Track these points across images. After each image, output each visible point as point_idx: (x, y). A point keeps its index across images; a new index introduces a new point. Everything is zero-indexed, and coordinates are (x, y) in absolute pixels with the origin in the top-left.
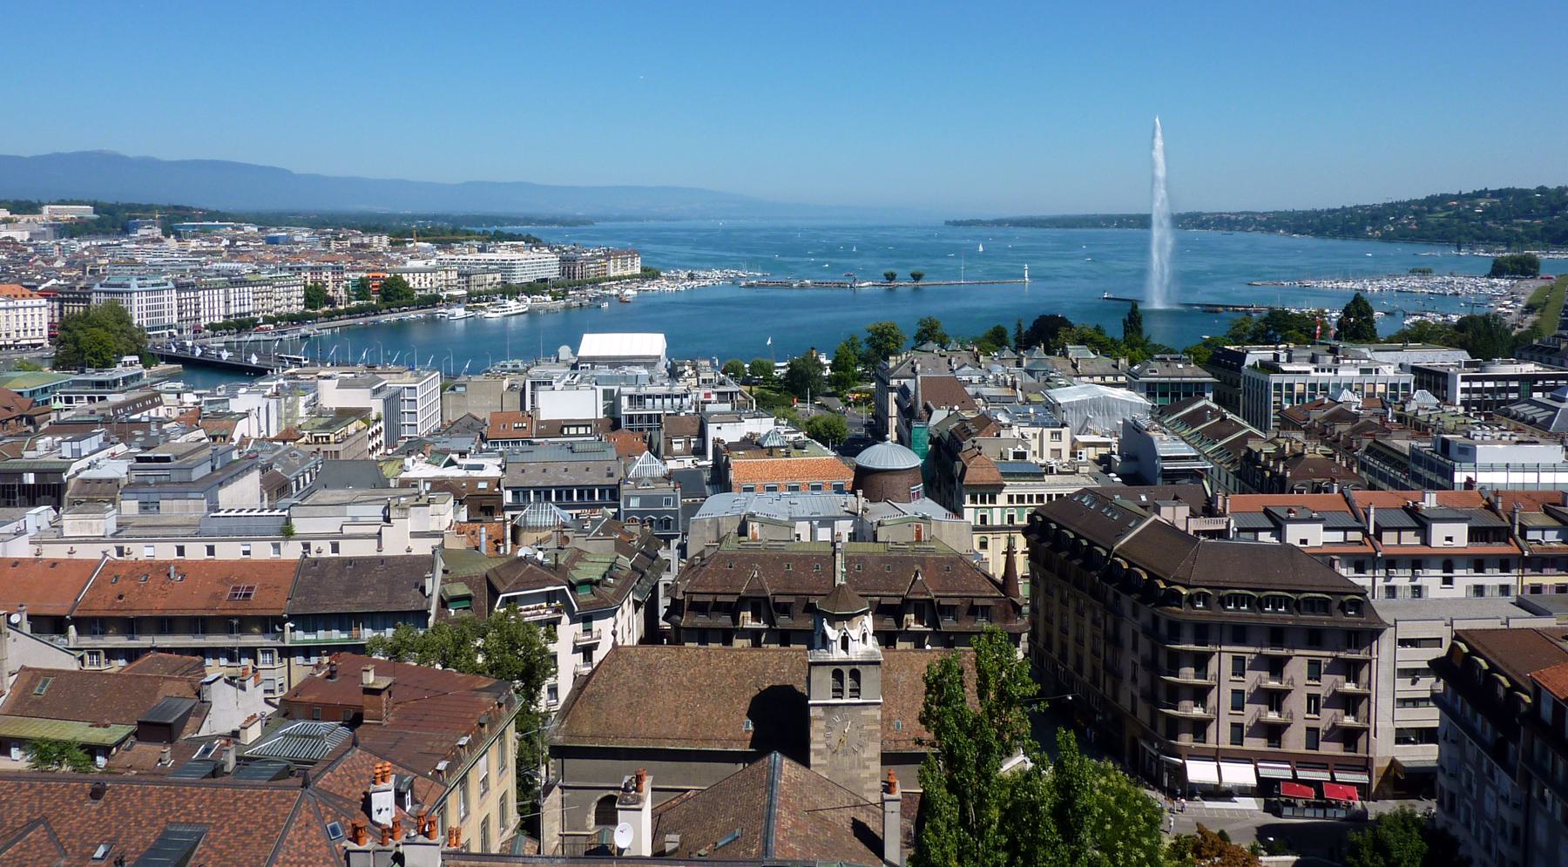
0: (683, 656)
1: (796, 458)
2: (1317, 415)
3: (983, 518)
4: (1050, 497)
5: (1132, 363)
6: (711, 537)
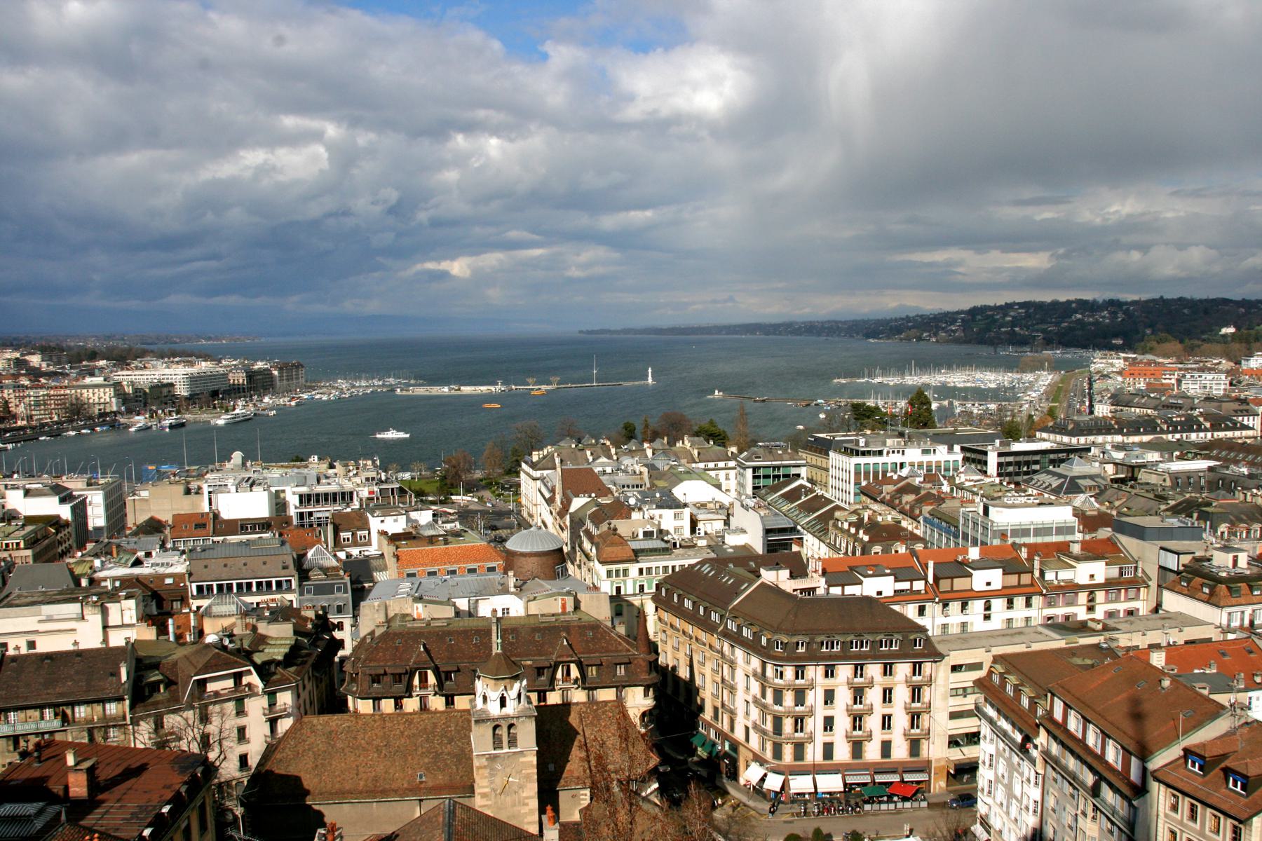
0: (360, 722)
1: (454, 545)
2: (888, 489)
3: (618, 589)
4: (673, 567)
5: (740, 452)
6: (381, 618)
